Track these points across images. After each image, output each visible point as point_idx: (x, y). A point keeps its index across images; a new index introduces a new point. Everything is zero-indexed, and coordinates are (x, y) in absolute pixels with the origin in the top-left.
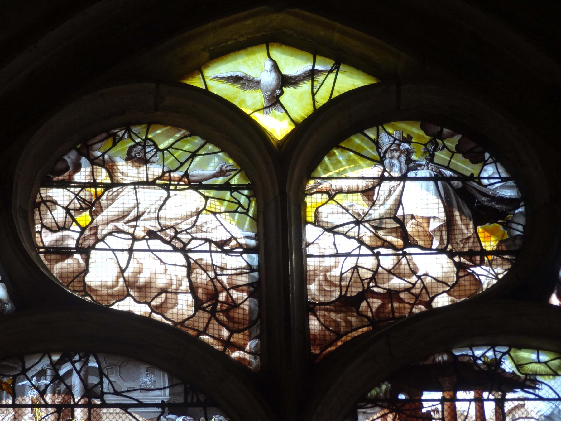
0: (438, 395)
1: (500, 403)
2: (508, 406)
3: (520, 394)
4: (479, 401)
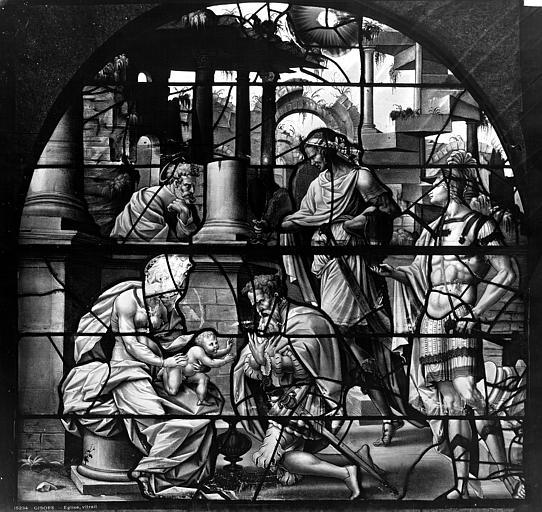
0: (190, 77)
1: (269, 89)
2: (281, 92)
3: (298, 74)
4: (243, 86)
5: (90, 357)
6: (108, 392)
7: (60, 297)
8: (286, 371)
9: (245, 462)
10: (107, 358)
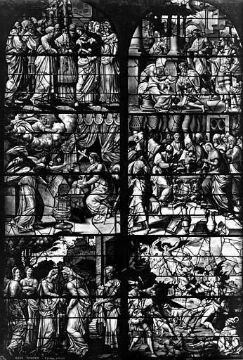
5: (144, 81)
6: (148, 89)
7: (137, 68)
8: (188, 84)
9: (179, 104)
10: (148, 81)
